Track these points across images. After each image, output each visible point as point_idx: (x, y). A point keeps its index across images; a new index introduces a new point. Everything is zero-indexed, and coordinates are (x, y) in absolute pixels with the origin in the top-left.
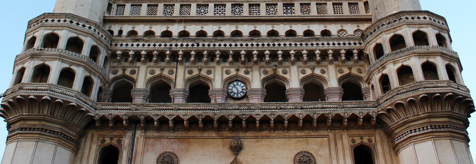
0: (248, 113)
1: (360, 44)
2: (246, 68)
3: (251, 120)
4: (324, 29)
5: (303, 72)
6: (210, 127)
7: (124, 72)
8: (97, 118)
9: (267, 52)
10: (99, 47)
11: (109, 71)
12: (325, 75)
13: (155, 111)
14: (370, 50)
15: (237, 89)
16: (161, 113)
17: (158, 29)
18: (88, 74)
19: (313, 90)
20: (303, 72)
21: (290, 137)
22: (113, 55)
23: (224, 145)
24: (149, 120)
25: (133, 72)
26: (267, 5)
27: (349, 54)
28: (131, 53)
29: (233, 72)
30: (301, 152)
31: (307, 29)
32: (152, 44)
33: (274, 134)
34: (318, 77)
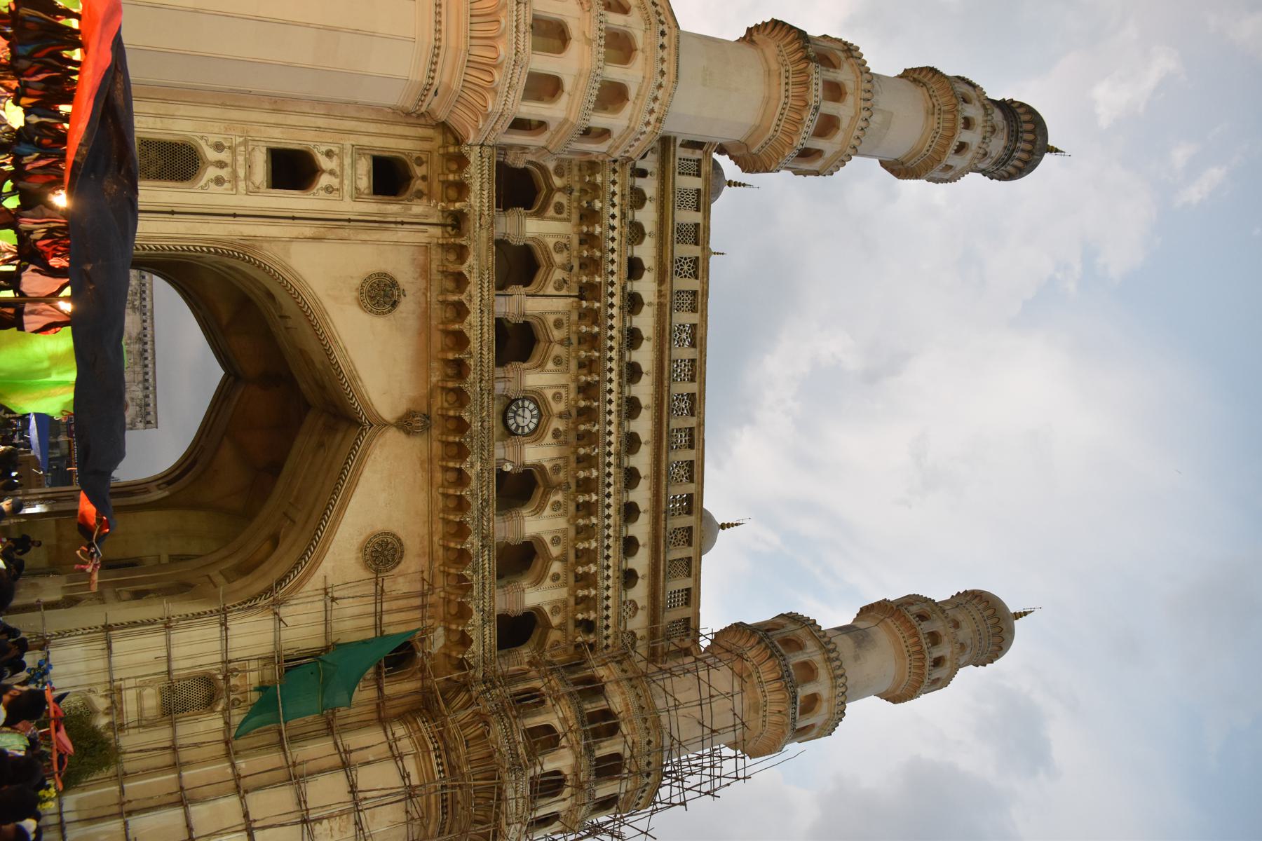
1: (607, 646)
2: (566, 431)
3: (461, 452)
4: (640, 575)
5: (556, 541)
6: (449, 371)
7: (559, 190)
8: (465, 149)
10: (610, 142)
11: (563, 160)
12: (548, 582)
15: (526, 419)
16: (474, 279)
17: (646, 252)
18: (553, 127)
19: (521, 559)
20: (556, 541)
21: (430, 523)
22: (592, 166)
23: (414, 400)
24: (461, 253)
25: (559, 208)
26: (692, 462)
27: (588, 626)
30: (401, 545)
31: (641, 543)
32: (615, 245)
33: (437, 494)
34: (546, 568)
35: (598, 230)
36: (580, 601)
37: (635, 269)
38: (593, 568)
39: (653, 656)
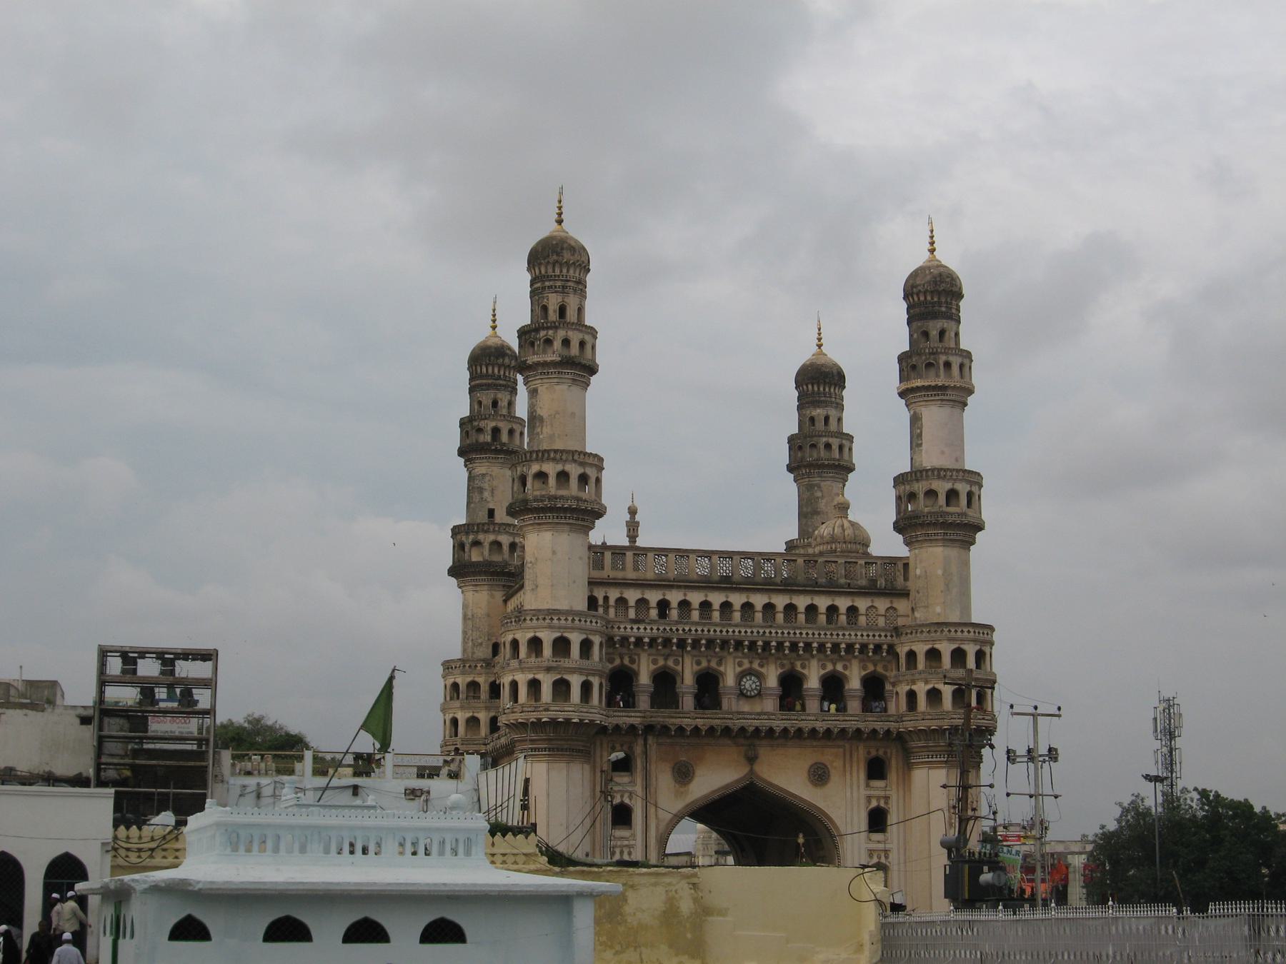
0: (768, 723)
3: (771, 730)
5: (824, 667)
9: (787, 644)
12: (847, 673)
13: (672, 720)
14: (902, 651)
15: (749, 683)
16: (677, 721)
17: (654, 597)
19: (833, 687)
20: (824, 667)
24: (665, 729)
25: (632, 661)
27: (878, 648)
28: (632, 639)
29: (746, 665)
35: (646, 640)
36: (861, 651)
37: (663, 606)
38: (843, 646)
39: (905, 594)
